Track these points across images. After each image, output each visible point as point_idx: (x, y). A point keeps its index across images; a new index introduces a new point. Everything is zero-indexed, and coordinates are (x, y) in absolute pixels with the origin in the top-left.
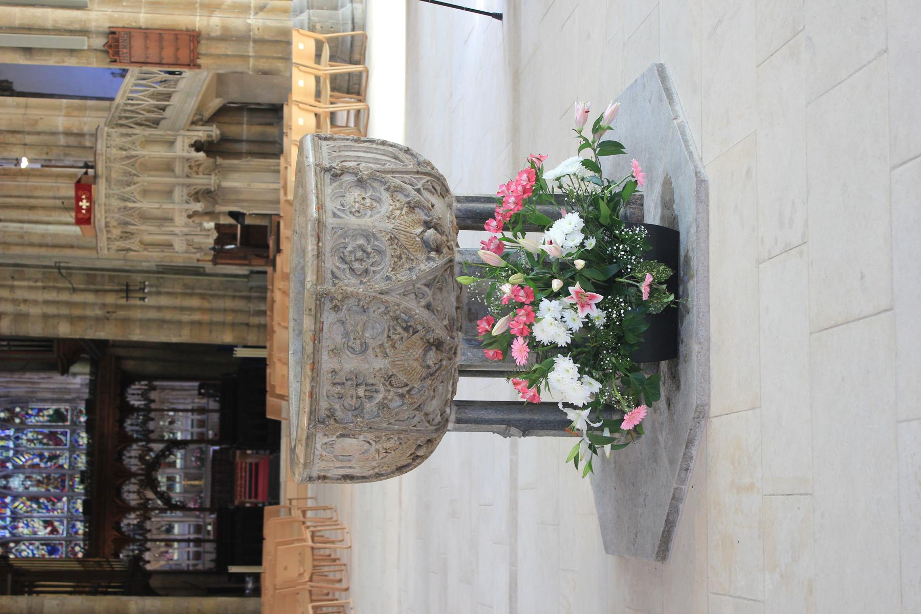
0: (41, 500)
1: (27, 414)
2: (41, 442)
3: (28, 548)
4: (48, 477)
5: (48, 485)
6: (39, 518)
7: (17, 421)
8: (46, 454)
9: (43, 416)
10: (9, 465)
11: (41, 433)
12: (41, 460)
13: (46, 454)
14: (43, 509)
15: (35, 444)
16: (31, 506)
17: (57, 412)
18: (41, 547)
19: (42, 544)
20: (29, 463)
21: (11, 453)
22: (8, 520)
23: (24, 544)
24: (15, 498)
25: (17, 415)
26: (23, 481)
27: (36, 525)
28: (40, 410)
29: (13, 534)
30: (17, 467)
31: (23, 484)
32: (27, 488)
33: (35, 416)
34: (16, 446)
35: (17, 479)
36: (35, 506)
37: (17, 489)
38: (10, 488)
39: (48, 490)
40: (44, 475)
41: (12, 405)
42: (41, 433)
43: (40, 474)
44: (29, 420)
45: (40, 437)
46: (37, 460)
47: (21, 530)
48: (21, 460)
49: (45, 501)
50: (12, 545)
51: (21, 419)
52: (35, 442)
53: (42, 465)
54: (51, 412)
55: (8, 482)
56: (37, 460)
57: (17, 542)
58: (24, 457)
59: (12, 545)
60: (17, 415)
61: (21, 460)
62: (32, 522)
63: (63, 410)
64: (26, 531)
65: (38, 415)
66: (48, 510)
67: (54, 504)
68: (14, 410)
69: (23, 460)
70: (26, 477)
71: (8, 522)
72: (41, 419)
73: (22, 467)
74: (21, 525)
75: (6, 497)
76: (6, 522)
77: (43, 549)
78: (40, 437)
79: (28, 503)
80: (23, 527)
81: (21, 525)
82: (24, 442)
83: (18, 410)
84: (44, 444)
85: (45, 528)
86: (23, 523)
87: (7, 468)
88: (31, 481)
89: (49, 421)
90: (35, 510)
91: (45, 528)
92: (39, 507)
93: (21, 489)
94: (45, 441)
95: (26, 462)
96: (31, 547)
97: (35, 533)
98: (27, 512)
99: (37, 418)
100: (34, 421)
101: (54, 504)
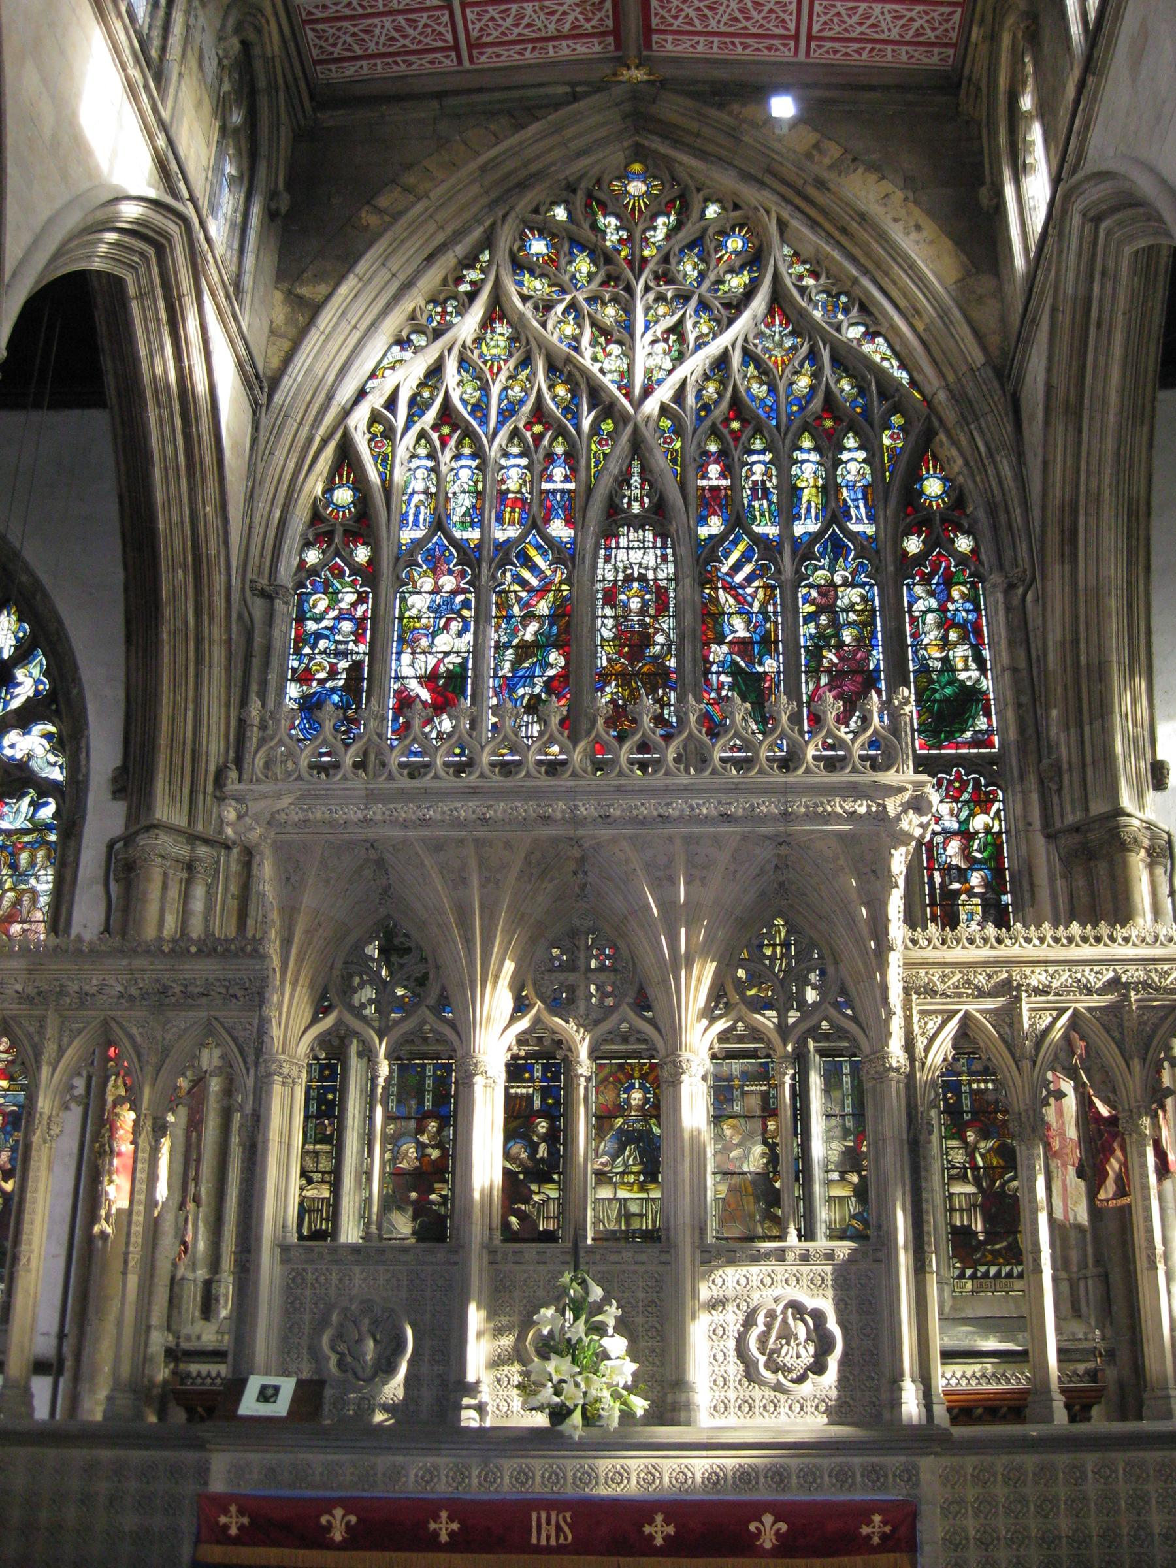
0: (554, 656)
1: (948, 582)
2: (821, 641)
3: (338, 619)
4: (658, 678)
5: (625, 678)
6: (477, 650)
7: (913, 545)
8: (770, 665)
9: (945, 644)
10: (714, 526)
11: (864, 642)
12: (741, 646)
13: (770, 665)
14: (513, 669)
15: (811, 617)
16: (529, 617)
17: (970, 698)
18: (343, 665)
19: (357, 666)
20: (726, 600)
21: (768, 530)
22: (473, 535)
23: (361, 599)
24: (562, 555)
25: (937, 542)
26: (642, 578)
27: (444, 642)
28: (971, 633)
29: (407, 558)
30: (713, 549)
31: (629, 579)
32: (610, 598)
33: (943, 609)
34: (804, 551)
35: (650, 559)
36: (530, 631)
37: (607, 559)
38: (609, 533)
39: (604, 677)
40: (672, 663)
41: (981, 515)
42: (864, 642)
43: (677, 645)
44: (919, 590)
45: (847, 636)
46: (739, 628)
47: (427, 583)
48: (736, 568)
49: (551, 672)
50: (362, 554)
51: (920, 558)
52: (823, 619)
53: (718, 652)
54: (969, 675)
55: (638, 523)
56: (739, 628)
57: (369, 574)
58: (749, 579)
59: (362, 554)
60: (937, 542)
61: (736, 568)
62: (455, 626)
63: (982, 723)
64: (419, 603)
65: (945, 624)
66: (509, 685)
67: (534, 706)
68: (960, 529)
69: (739, 578)
70: (661, 594)
71: (458, 535)
72: (931, 636)
73: (706, 579)
74: (448, 583)
75: (569, 522)
76: (464, 526)
77: (333, 673)
78: (847, 636)
79: (543, 608)
80: (436, 591)
81: (448, 583)
82: (820, 576)
83: (964, 544)
84: (815, 654)
85: (429, 680)
86: (454, 593)
87: (703, 520)
88: (643, 612)
89: (924, 670)
90: (514, 632)
91: (429, 680)
92: (524, 650)
93: (605, 572)
94: (830, 656)
95: (730, 588)
96: (347, 626)
97: (407, 640)
98: (504, 605)
99: (930, 618)
100: (920, 606)
101: (534, 706)
